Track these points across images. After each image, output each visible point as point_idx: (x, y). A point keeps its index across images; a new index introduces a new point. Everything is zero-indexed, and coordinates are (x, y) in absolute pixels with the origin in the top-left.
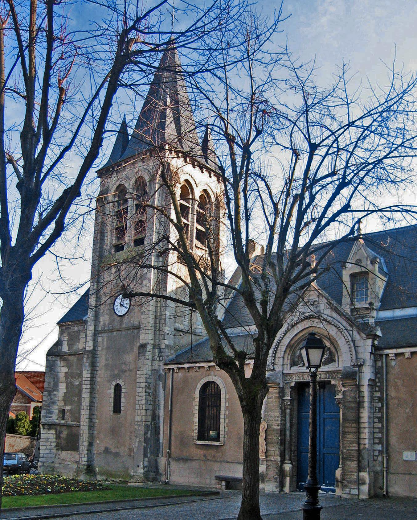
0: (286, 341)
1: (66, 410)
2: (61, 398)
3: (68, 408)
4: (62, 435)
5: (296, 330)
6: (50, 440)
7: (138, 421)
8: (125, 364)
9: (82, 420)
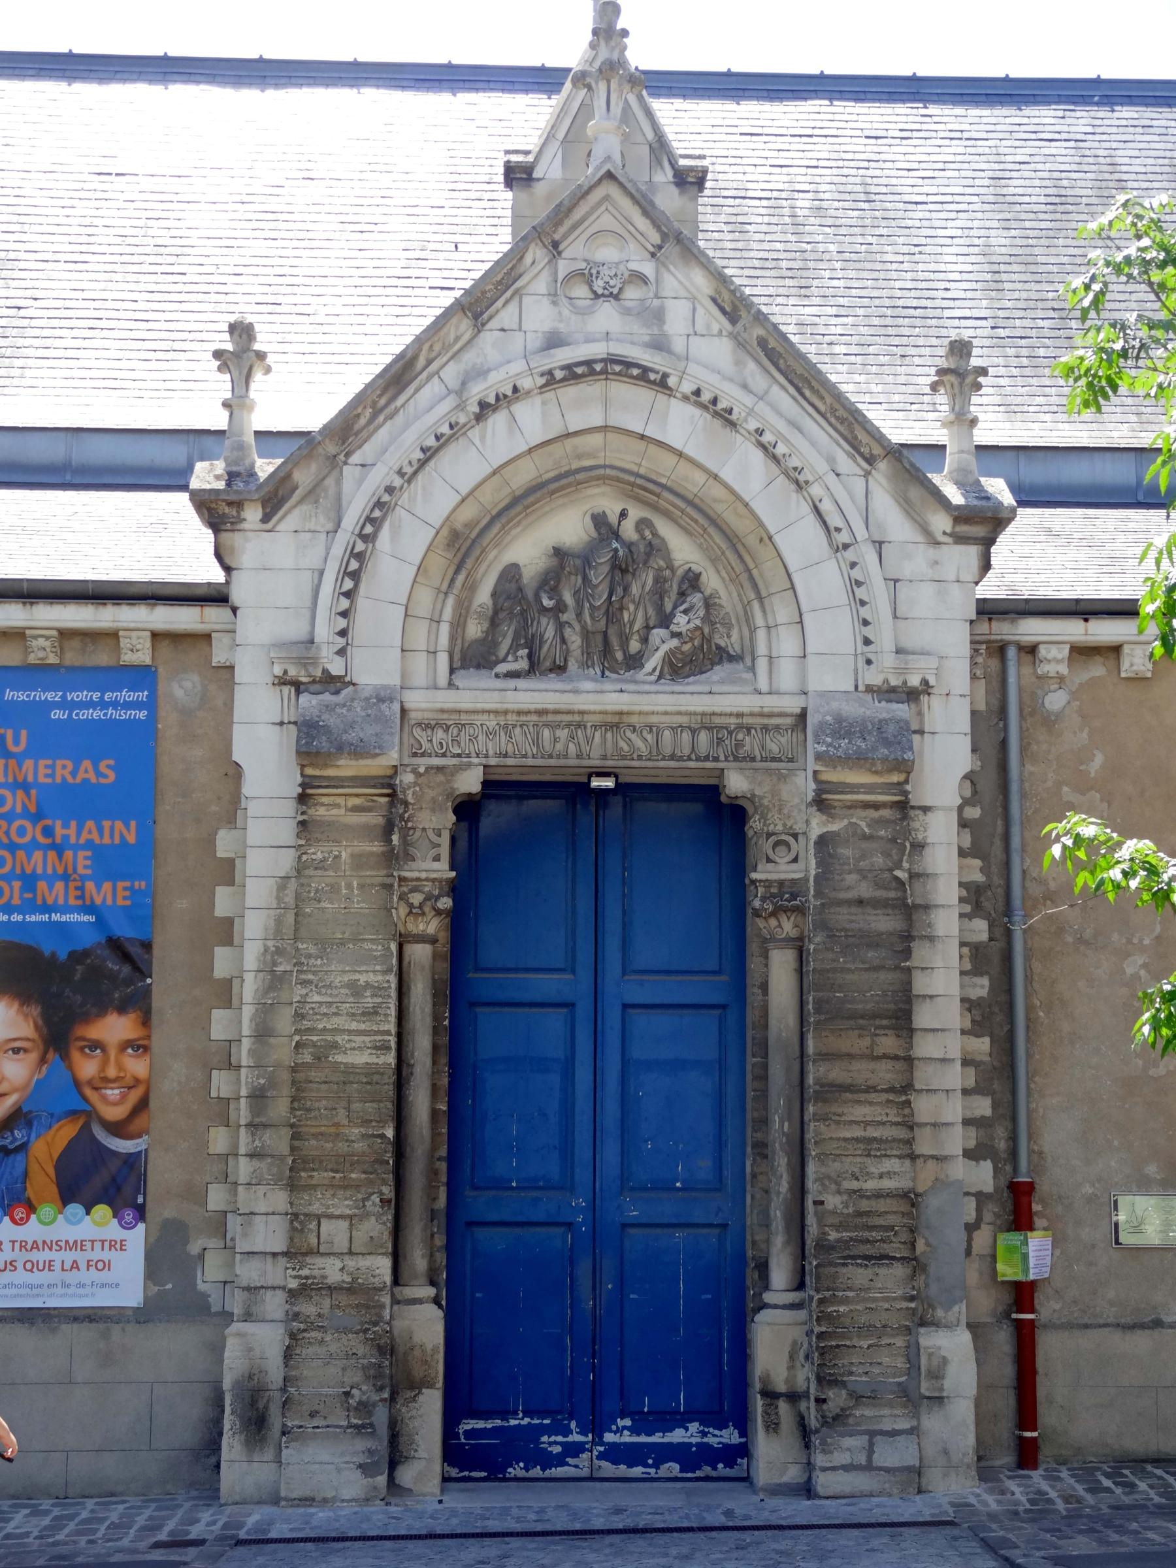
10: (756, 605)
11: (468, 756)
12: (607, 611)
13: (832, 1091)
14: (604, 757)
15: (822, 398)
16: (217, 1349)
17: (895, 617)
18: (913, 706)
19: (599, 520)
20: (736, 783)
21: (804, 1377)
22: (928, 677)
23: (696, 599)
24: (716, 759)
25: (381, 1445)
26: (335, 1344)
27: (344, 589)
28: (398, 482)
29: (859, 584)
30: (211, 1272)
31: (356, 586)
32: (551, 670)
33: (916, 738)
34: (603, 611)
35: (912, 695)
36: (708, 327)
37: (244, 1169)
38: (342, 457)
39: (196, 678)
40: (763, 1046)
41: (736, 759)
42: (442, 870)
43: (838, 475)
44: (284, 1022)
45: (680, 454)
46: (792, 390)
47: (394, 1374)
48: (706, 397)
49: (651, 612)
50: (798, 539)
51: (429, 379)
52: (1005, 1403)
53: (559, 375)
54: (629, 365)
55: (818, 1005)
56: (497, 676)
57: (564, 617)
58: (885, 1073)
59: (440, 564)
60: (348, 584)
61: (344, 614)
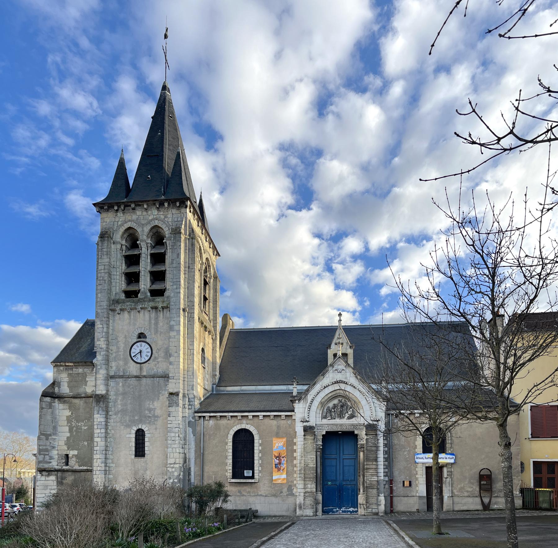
1: (70, 456)
2: (62, 443)
3: (72, 453)
4: (64, 481)
5: (327, 391)
6: (49, 487)
7: (171, 464)
8: (150, 410)
9: (95, 464)
13: (367, 469)
16: (295, 500)
19: (339, 400)
20: (356, 432)
21: (364, 502)
25: (315, 510)
26: (309, 498)
30: (295, 490)
35: (378, 421)
37: (298, 479)
40: (359, 463)
42: (321, 443)
44: (303, 462)
47: (317, 503)
50: (363, 402)
52: (389, 505)
55: (367, 459)
58: (374, 467)
59: (320, 406)
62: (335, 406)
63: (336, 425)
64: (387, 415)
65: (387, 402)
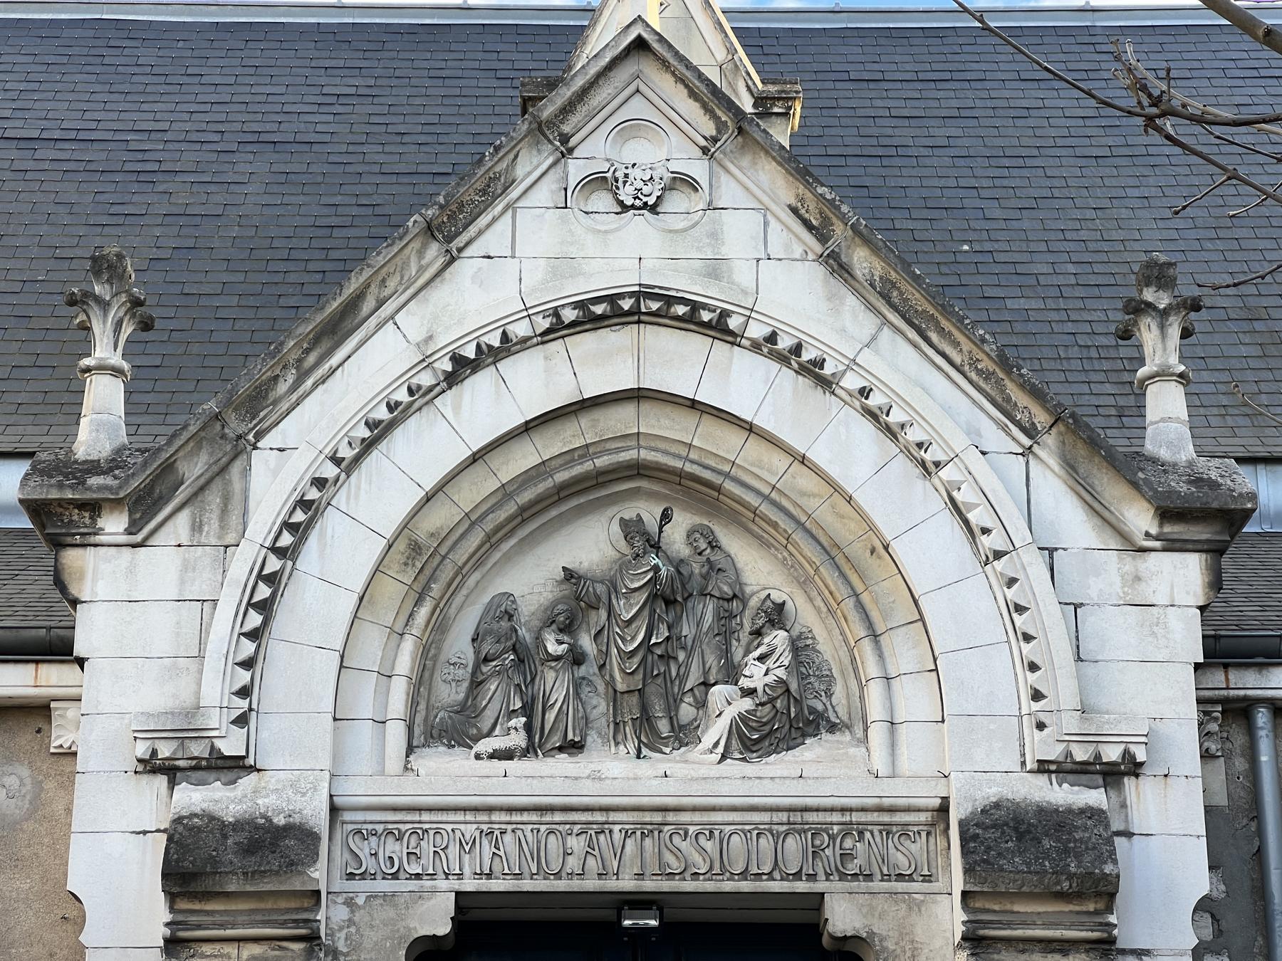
0: (381, 500)
5: (488, 406)
10: (867, 645)
11: (432, 876)
12: (643, 661)
14: (640, 876)
15: (956, 344)
17: (1079, 659)
18: (1112, 794)
19: (632, 529)
20: (843, 916)
22: (1133, 748)
23: (778, 638)
24: (812, 877)
27: (248, 627)
28: (330, 471)
29: (1020, 609)
31: (266, 623)
32: (561, 749)
33: (1118, 841)
34: (636, 660)
35: (1114, 774)
36: (787, 247)
38: (251, 437)
39: (25, 772)
41: (843, 877)
43: (984, 453)
45: (750, 428)
46: (912, 334)
48: (784, 343)
49: (711, 660)
50: (928, 550)
51: (380, 326)
53: (569, 315)
54: (670, 300)
56: (478, 757)
57: (582, 671)
59: (392, 591)
60: (255, 619)
61: (248, 664)
62: (579, 599)
63: (593, 817)
64: (1227, 716)
65: (1215, 551)
